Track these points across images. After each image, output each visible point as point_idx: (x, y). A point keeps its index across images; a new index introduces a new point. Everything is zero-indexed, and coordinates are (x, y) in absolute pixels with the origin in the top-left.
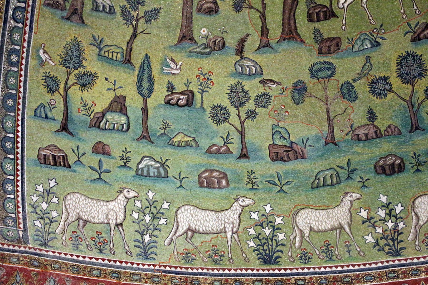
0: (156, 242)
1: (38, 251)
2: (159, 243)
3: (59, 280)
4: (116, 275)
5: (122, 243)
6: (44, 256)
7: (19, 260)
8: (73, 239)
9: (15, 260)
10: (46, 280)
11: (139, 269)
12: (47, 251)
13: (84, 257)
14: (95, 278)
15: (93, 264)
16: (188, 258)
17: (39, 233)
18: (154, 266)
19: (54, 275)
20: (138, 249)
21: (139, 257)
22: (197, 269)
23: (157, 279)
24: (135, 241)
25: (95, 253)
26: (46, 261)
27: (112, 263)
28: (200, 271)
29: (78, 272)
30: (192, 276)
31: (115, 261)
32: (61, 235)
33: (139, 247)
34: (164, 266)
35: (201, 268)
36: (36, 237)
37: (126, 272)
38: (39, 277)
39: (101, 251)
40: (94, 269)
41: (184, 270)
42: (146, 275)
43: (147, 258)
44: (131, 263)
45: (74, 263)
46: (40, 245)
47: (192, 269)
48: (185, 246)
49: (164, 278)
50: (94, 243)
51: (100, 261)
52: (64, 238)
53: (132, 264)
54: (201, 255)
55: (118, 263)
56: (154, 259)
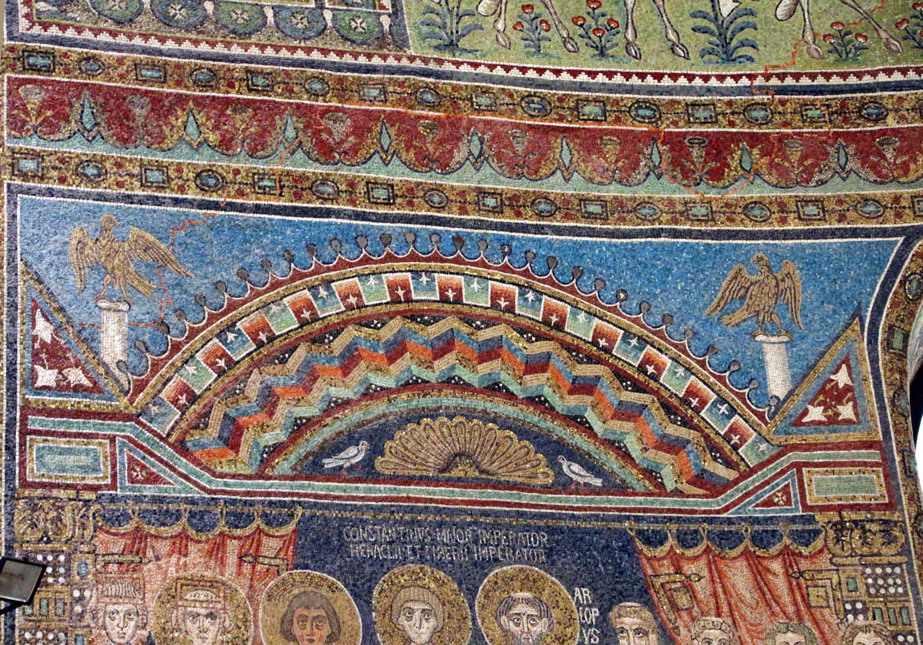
0: (752, 13)
1: (432, 66)
2: (761, 16)
3: (493, 138)
4: (648, 113)
5: (657, 24)
6: (450, 76)
7: (384, 92)
8: (526, 25)
9: (375, 93)
10: (459, 139)
11: (709, 90)
12: (458, 64)
13: (557, 72)
14: (591, 126)
15: (582, 87)
16: (845, 46)
17: (434, 16)
18: (751, 77)
19: (481, 125)
20: (703, 37)
21: (707, 57)
22: (874, 74)
23: (762, 113)
24: (694, 16)
25: (586, 60)
26: (455, 88)
27: (635, 81)
28: (882, 78)
29: (544, 112)
30: (859, 95)
31: (642, 76)
32: (492, 19)
33: (705, 31)
34: (778, 75)
35: (884, 71)
36: (425, 29)
37: (673, 102)
38: (440, 133)
39: (602, 53)
40: (587, 100)
41: (835, 81)
42: (730, 104)
43: (729, 58)
44: (686, 75)
45: (532, 90)
46: (437, 48)
47: (859, 75)
48: (836, 14)
49: (780, 109)
50: (581, 31)
51: (601, 78)
52: (500, 26)
53: (690, 78)
54: (883, 35)
55: (650, 81)
56: (751, 59)
